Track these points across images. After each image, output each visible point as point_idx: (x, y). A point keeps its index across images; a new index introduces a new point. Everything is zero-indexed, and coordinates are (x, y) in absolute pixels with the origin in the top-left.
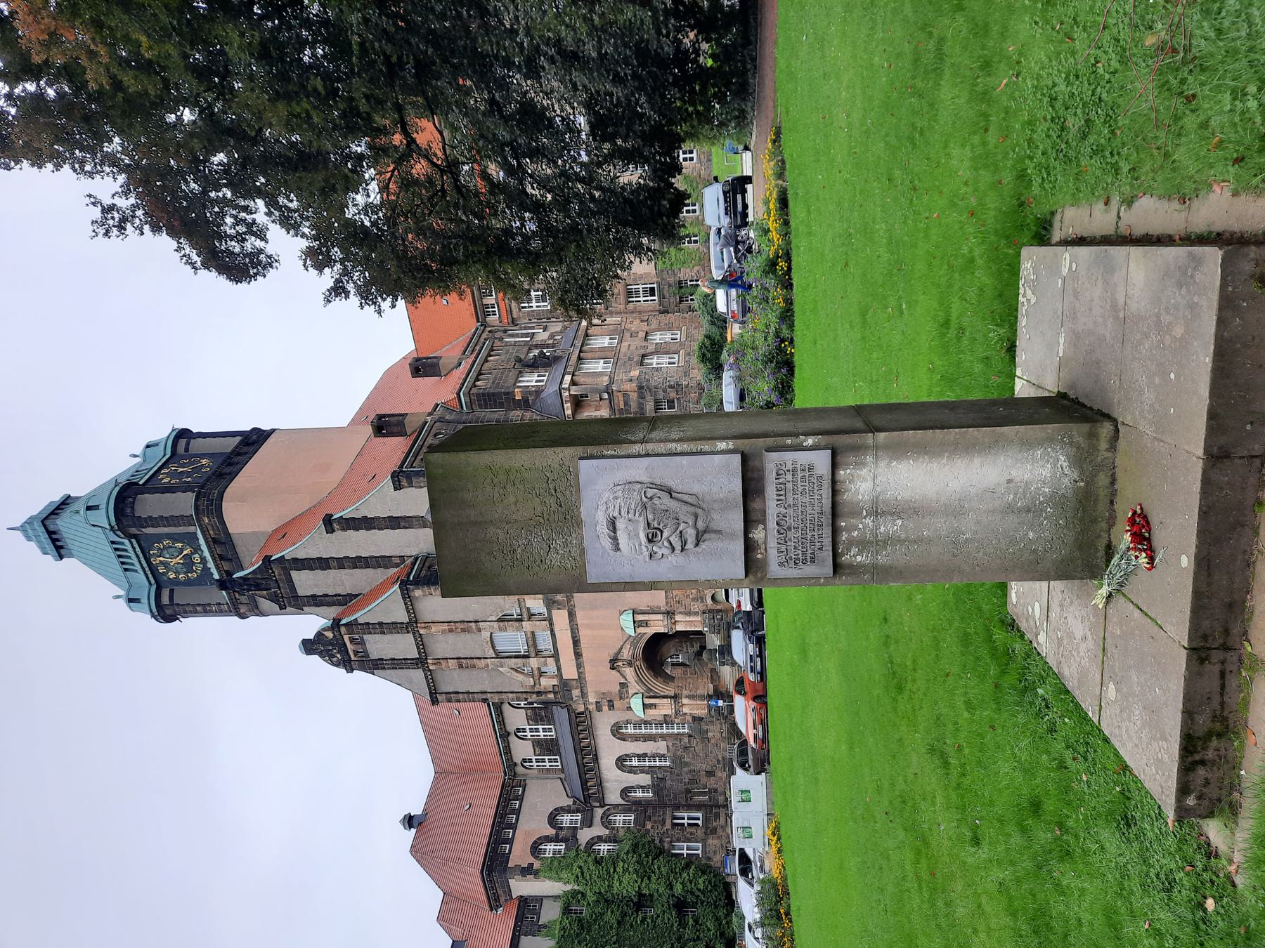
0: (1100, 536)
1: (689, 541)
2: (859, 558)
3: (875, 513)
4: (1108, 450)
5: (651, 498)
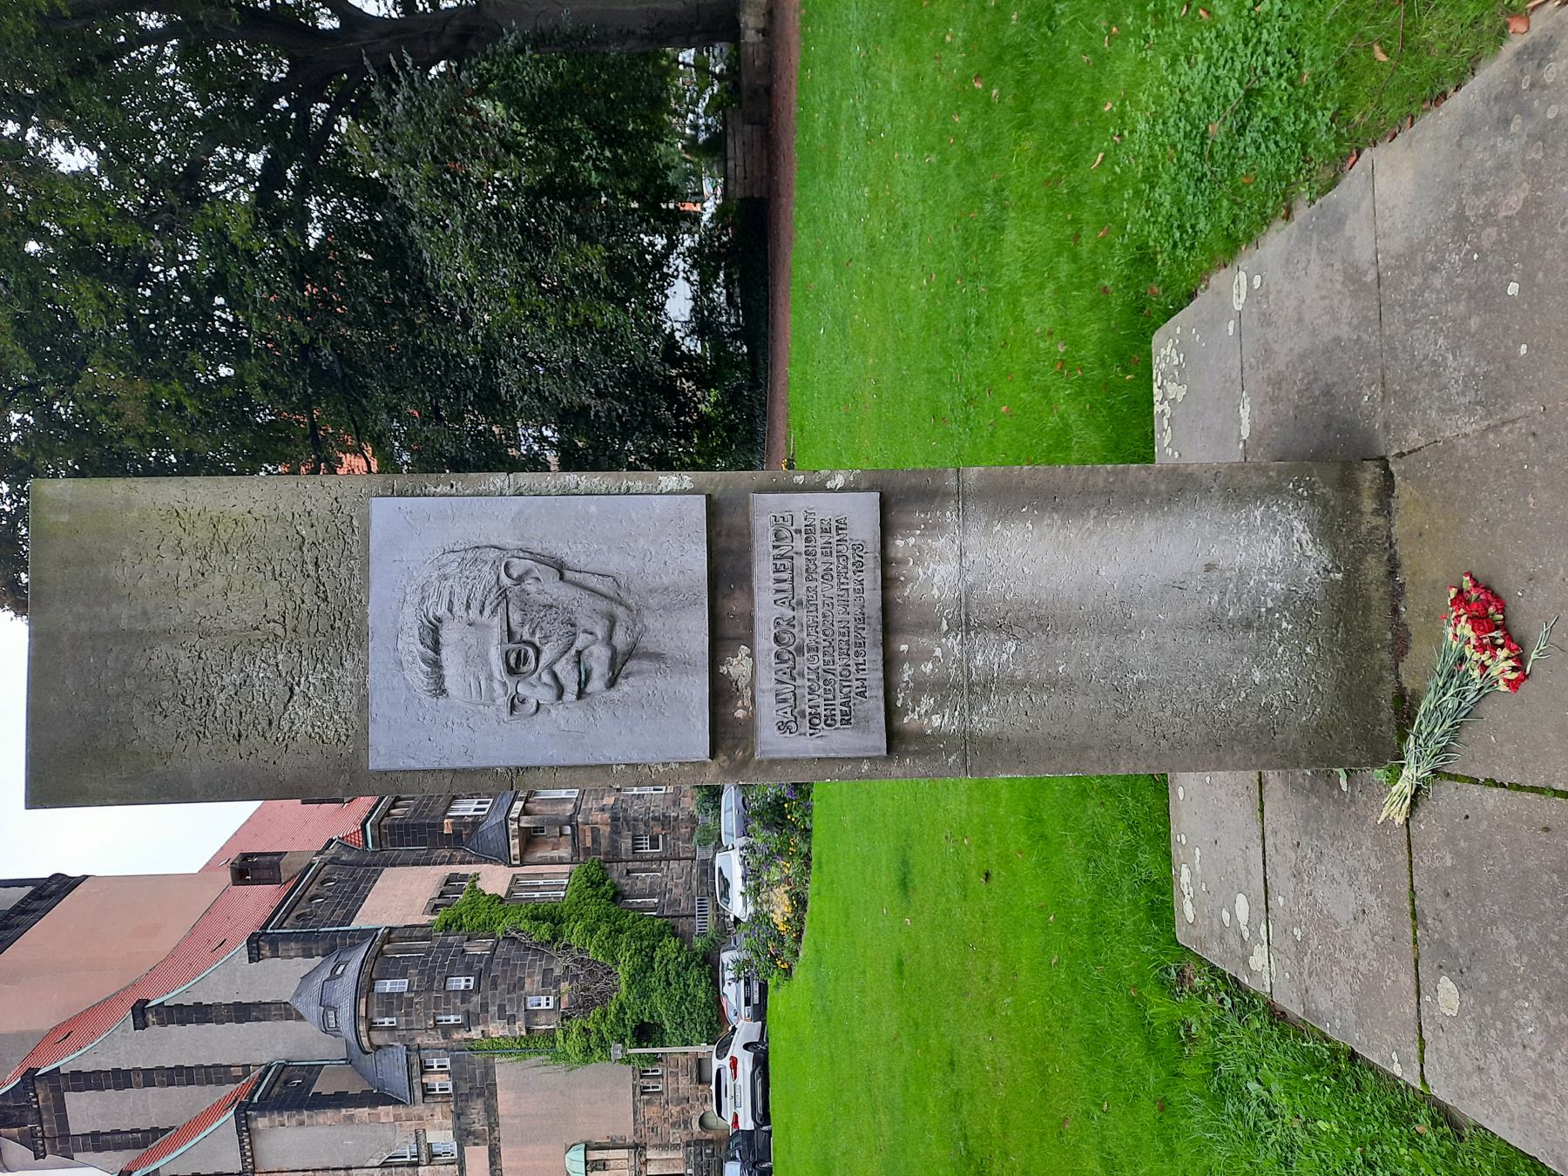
0: (1381, 679)
1: (595, 675)
2: (936, 720)
3: (965, 626)
4: (1376, 512)
5: (520, 580)
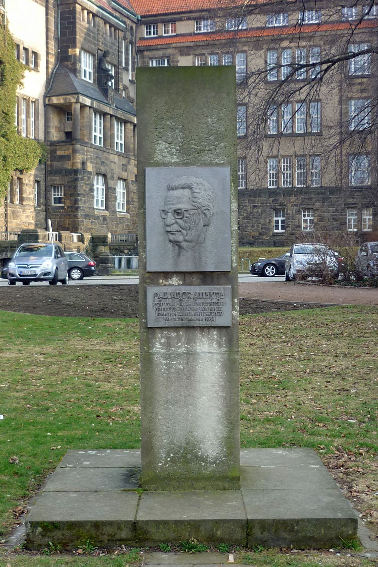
1: (174, 236)
